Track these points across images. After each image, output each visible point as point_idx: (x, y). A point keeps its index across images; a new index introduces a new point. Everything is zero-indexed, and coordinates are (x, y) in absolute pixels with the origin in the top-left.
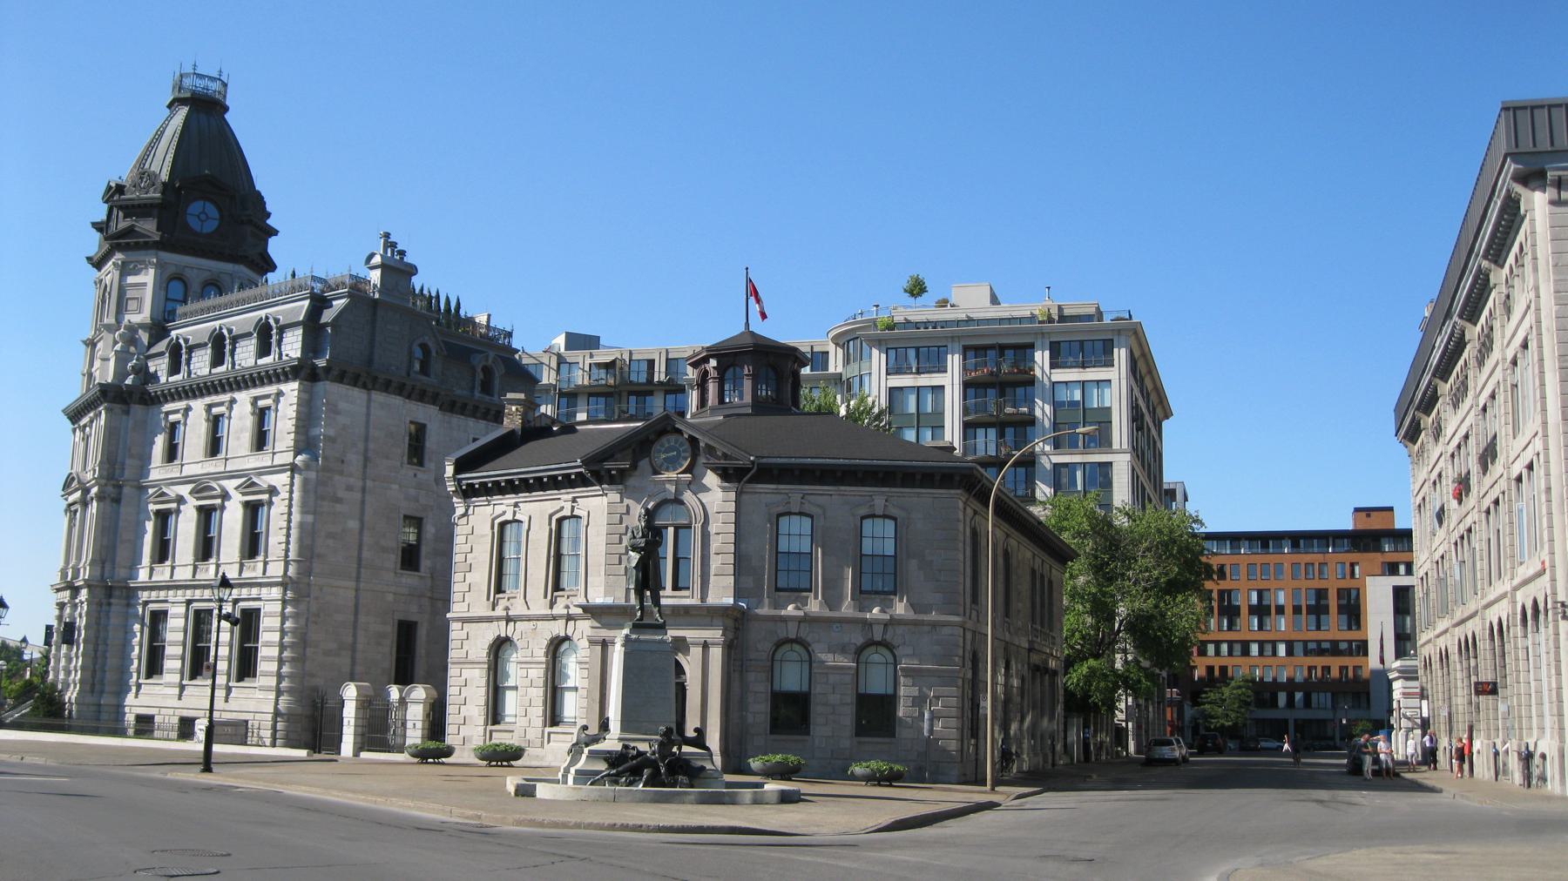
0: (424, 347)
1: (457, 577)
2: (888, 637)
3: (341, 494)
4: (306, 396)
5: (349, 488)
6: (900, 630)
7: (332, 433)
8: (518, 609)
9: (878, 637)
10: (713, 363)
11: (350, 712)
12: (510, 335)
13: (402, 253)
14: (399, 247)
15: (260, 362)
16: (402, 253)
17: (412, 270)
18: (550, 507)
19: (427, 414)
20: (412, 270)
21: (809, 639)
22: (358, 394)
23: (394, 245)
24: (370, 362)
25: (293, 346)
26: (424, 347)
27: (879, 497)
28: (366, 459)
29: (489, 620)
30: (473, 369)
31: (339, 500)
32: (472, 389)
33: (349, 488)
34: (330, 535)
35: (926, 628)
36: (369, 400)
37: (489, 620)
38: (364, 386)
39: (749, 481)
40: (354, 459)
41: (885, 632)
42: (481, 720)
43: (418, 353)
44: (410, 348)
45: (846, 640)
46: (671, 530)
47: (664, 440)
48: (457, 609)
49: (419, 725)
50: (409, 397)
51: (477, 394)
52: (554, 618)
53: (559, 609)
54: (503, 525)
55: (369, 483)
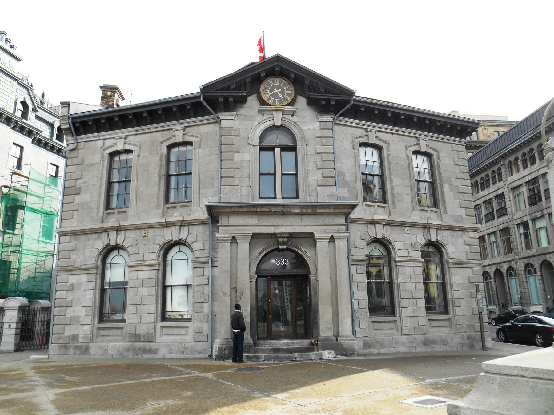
0: (24, 103)
2: (440, 239)
9: (434, 239)
18: (159, 136)
19: (26, 141)
21: (391, 239)
26: (24, 103)
29: (99, 231)
32: (52, 136)
37: (99, 231)
39: (341, 116)
41: (437, 236)
42: (89, 320)
43: (20, 107)
44: (16, 103)
45: (414, 240)
46: (278, 150)
49: (14, 326)
50: (13, 128)
51: (54, 139)
52: (168, 225)
54: (112, 155)
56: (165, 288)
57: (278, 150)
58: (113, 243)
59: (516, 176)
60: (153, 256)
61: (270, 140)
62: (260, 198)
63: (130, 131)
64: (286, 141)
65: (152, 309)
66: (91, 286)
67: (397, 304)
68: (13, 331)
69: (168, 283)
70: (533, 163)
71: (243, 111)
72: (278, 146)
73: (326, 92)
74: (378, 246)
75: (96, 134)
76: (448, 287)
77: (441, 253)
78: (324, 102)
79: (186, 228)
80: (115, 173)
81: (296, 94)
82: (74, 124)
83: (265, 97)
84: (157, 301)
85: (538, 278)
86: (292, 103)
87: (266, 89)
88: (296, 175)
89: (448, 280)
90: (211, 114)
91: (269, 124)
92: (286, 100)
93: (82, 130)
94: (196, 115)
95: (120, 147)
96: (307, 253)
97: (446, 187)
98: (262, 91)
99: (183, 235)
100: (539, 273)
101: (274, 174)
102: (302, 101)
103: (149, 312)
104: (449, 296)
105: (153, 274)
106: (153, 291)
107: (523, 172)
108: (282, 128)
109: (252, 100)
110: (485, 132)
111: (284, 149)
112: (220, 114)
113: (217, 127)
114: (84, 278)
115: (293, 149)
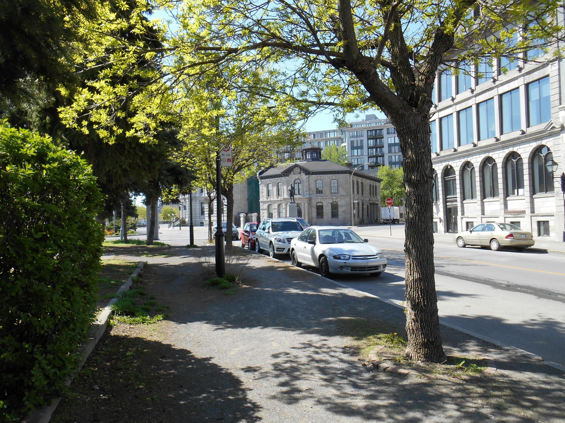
1: (260, 194)
8: (272, 199)
11: (242, 219)
27: (334, 176)
48: (261, 200)
53: (279, 199)
61: (296, 181)
64: (299, 181)
71: (290, 176)
86: (300, 173)
109: (292, 173)
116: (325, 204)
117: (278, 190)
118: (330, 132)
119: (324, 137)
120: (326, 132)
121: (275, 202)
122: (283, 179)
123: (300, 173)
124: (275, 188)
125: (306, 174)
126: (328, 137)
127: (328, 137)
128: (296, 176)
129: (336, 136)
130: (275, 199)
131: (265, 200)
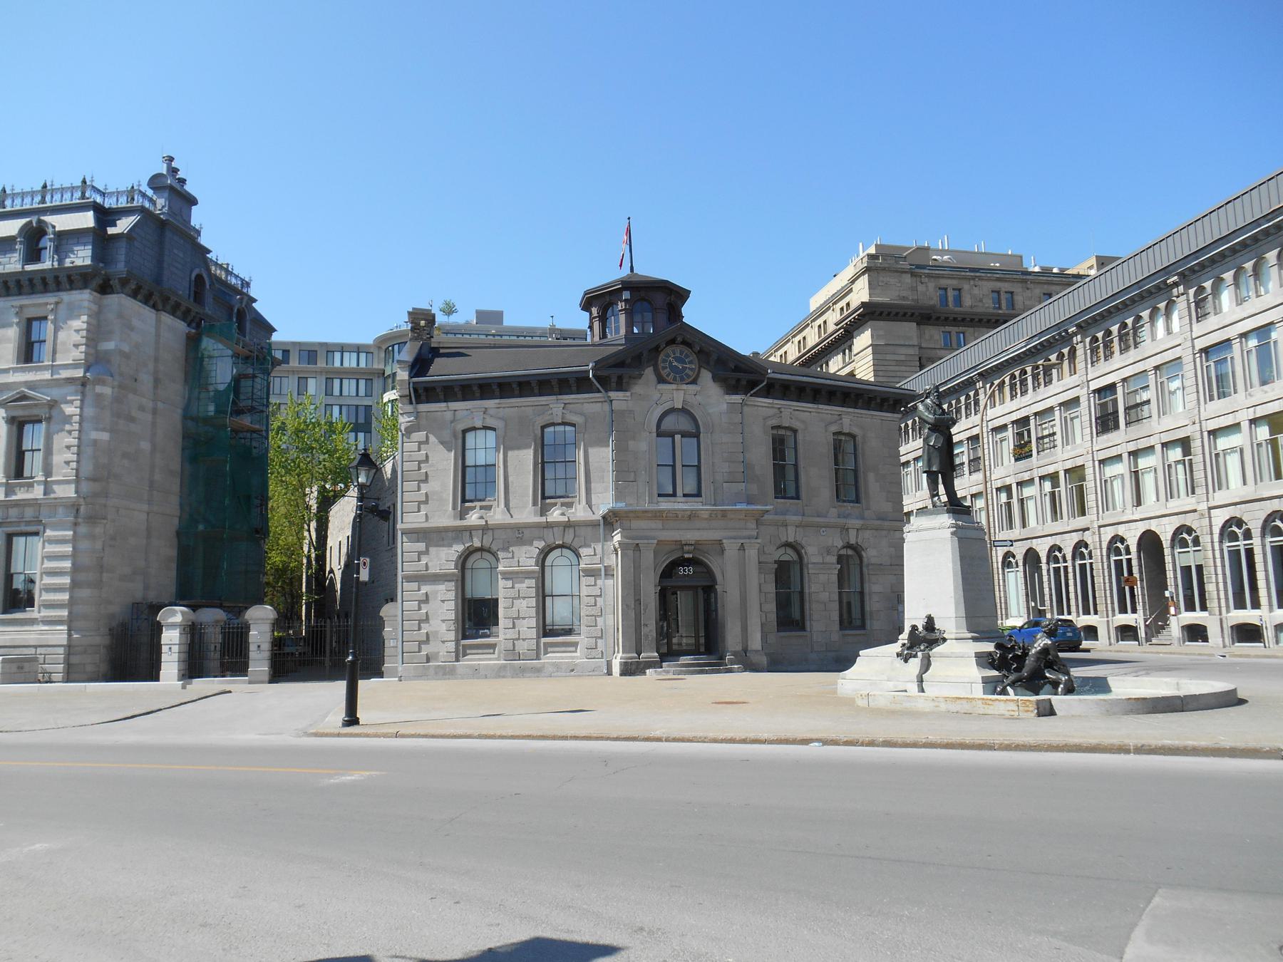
3: (134, 413)
4: (95, 308)
5: (142, 408)
6: (867, 534)
7: (126, 349)
8: (498, 516)
9: (853, 541)
10: (626, 295)
12: (248, 284)
13: (183, 181)
14: (180, 175)
15: (29, 268)
16: (183, 181)
17: (192, 201)
20: (192, 201)
21: (803, 543)
22: (147, 313)
23: (174, 171)
24: (158, 281)
25: (82, 257)
28: (157, 381)
30: (231, 308)
31: (132, 419)
33: (142, 408)
34: (125, 455)
35: (884, 533)
36: (158, 321)
38: (154, 307)
40: (146, 379)
42: (452, 636)
47: (669, 350)
54: (465, 432)
55: (160, 405)
56: (544, 597)
57: (678, 437)
58: (477, 544)
59: (999, 410)
60: (533, 562)
61: (669, 423)
62: (660, 495)
63: (491, 403)
64: (684, 424)
65: (533, 623)
66: (452, 595)
67: (807, 617)
68: (267, 654)
69: (548, 591)
70: (1024, 392)
71: (638, 388)
72: (678, 433)
73: (737, 369)
74: (789, 551)
75: (444, 405)
76: (867, 598)
77: (861, 557)
78: (733, 382)
79: (571, 530)
80: (469, 455)
81: (700, 367)
82: (416, 390)
83: (664, 373)
84: (537, 613)
85: (1021, 574)
87: (664, 361)
88: (698, 467)
89: (866, 590)
90: (599, 391)
91: (667, 406)
92: (688, 376)
93: (423, 398)
94: (579, 391)
95: (479, 424)
96: (714, 564)
97: (871, 477)
98: (661, 365)
99: (568, 539)
100: (1021, 568)
101: (674, 466)
102: (706, 376)
103: (528, 627)
104: (867, 608)
105: (532, 582)
106: (533, 602)
107: (1010, 405)
108: (684, 411)
109: (649, 373)
110: (976, 291)
111: (684, 435)
112: (613, 394)
113: (606, 407)
114: (441, 588)
115: (697, 435)
116: (812, 553)
117: (541, 466)
118: (343, 349)
119: (321, 364)
120: (330, 349)
121: (519, 534)
122: (588, 405)
123: (694, 382)
124: (524, 459)
125: (732, 388)
126: (337, 364)
127: (337, 364)
128: (676, 395)
129: (363, 365)
130: (526, 514)
131: (444, 517)
